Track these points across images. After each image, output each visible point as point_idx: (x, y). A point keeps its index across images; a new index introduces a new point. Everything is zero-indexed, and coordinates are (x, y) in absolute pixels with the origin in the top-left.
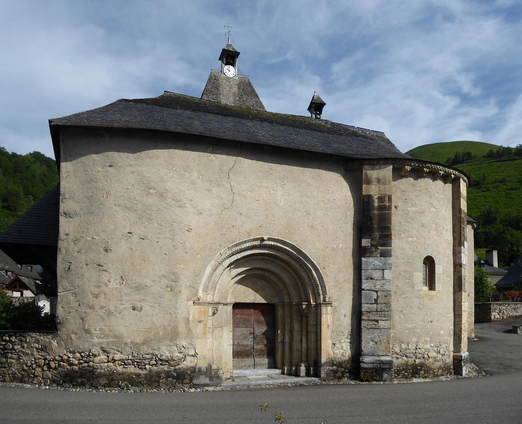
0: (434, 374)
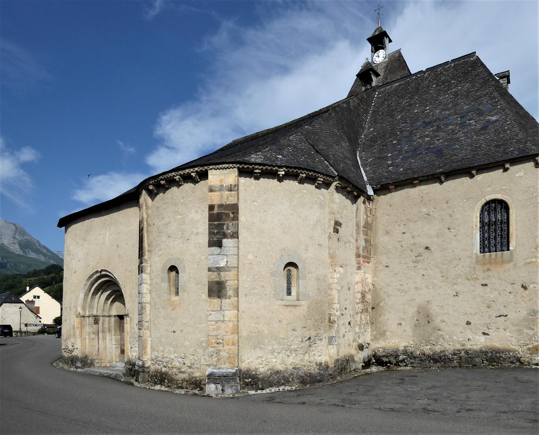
0: (177, 384)
